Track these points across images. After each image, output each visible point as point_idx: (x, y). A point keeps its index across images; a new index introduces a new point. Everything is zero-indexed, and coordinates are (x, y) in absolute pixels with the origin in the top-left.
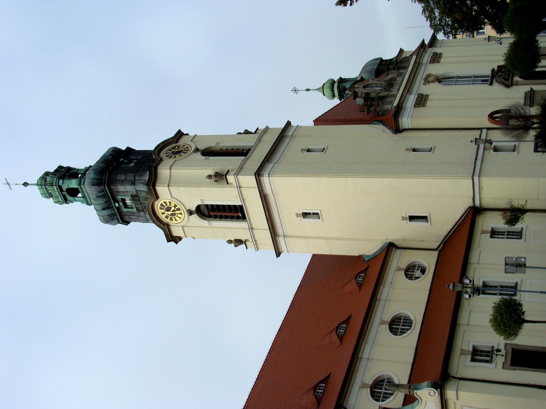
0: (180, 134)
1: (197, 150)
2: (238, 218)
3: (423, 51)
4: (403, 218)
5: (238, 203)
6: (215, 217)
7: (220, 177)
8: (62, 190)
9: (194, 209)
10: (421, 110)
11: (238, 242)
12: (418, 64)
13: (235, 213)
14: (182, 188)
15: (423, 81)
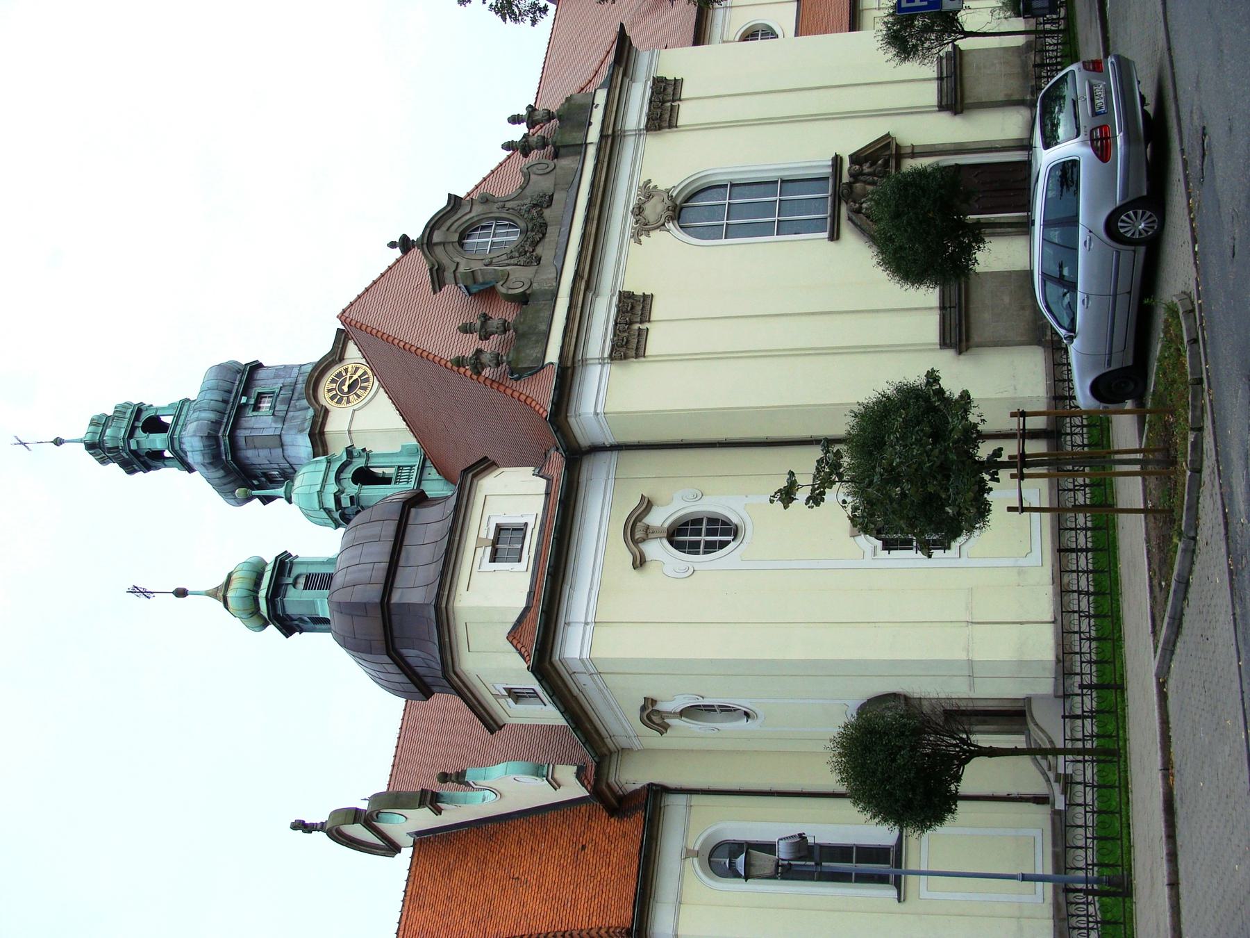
3: (625, 74)
10: (632, 375)
12: (612, 139)
15: (631, 219)
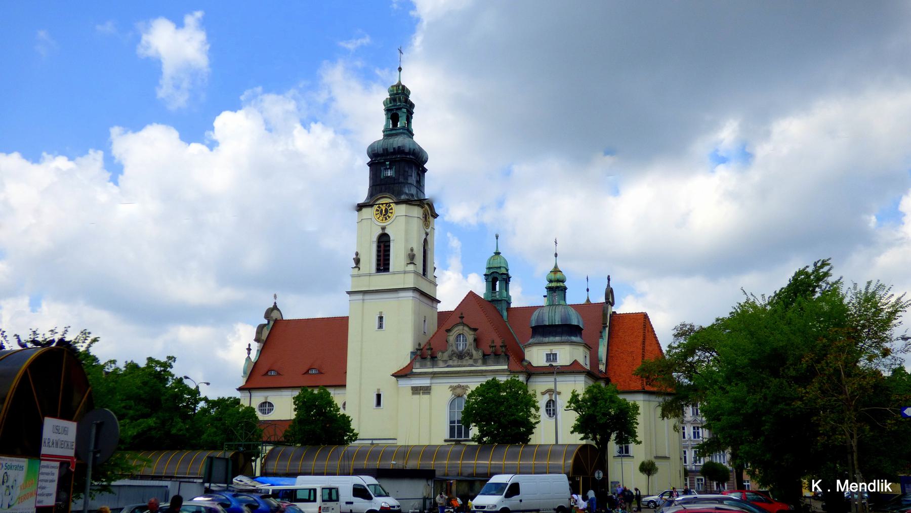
0: (435, 216)
1: (427, 234)
2: (378, 265)
4: (379, 390)
5: (392, 267)
6: (379, 247)
7: (411, 258)
8: (397, 109)
9: (387, 231)
11: (357, 261)
13: (383, 264)
14: (403, 224)
